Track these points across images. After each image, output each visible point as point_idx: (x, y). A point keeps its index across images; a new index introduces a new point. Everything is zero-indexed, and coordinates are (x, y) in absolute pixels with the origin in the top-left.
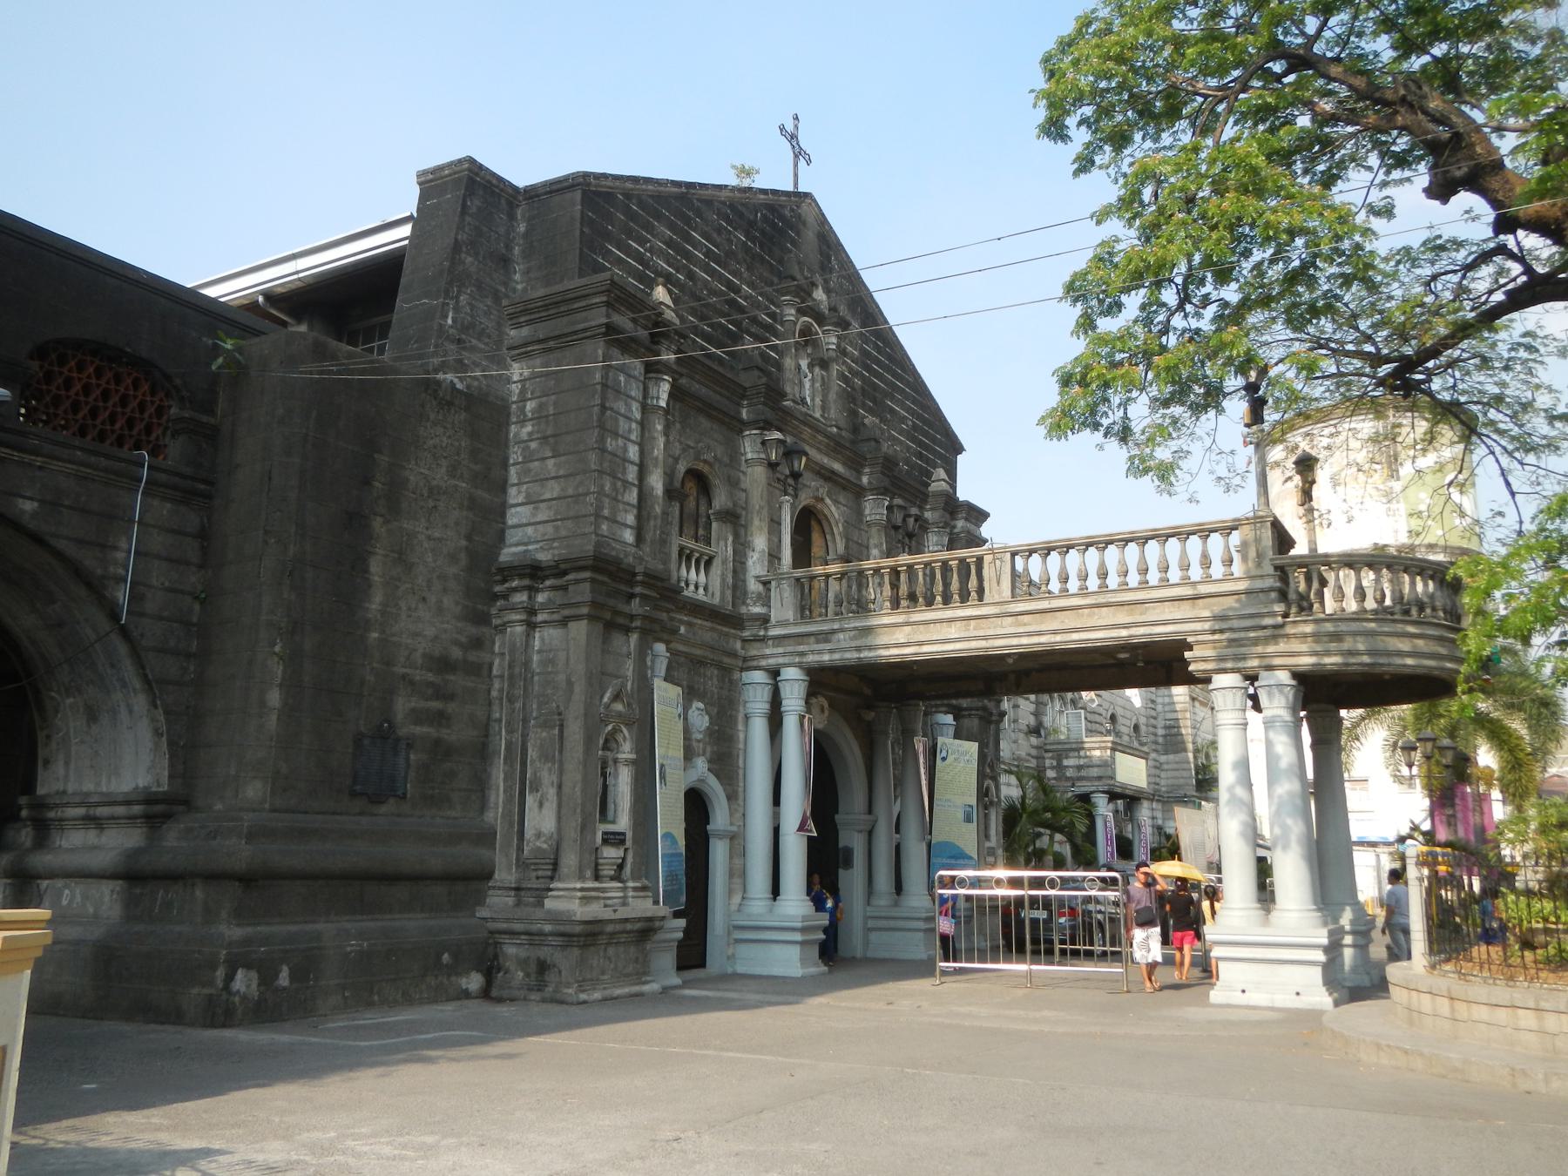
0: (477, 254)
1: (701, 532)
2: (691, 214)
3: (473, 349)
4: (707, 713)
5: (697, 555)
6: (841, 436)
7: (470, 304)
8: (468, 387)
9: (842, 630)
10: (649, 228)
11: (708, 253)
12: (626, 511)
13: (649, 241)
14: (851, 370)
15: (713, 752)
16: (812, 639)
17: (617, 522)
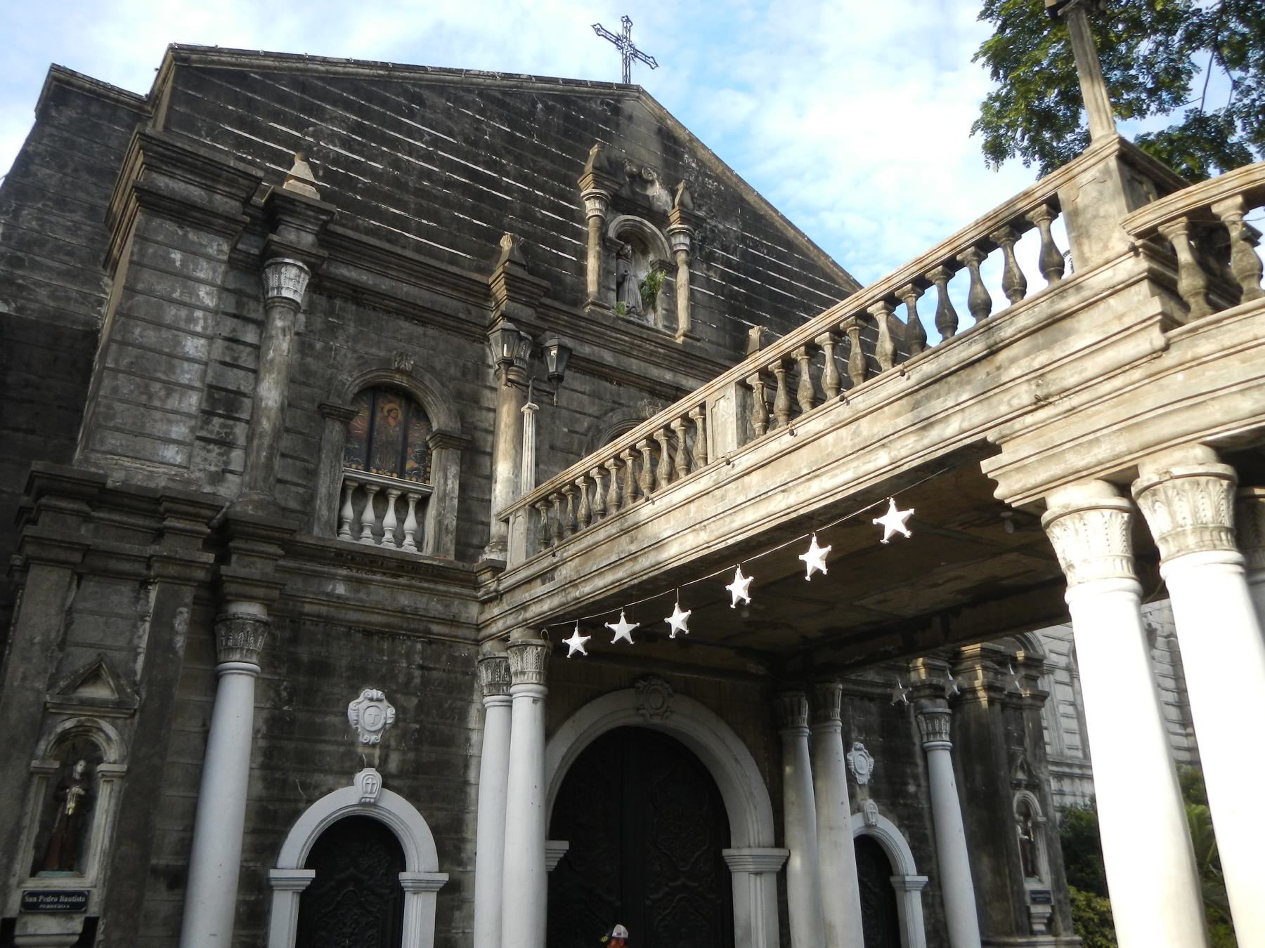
0: (61, 167)
1: (410, 464)
2: (401, 99)
3: (35, 266)
4: (392, 700)
5: (395, 493)
6: (693, 346)
7: (37, 219)
8: (19, 309)
9: (564, 562)
10: (320, 114)
11: (435, 142)
12: (170, 422)
13: (314, 125)
14: (724, 275)
15: (404, 762)
16: (539, 581)
17: (149, 436)
